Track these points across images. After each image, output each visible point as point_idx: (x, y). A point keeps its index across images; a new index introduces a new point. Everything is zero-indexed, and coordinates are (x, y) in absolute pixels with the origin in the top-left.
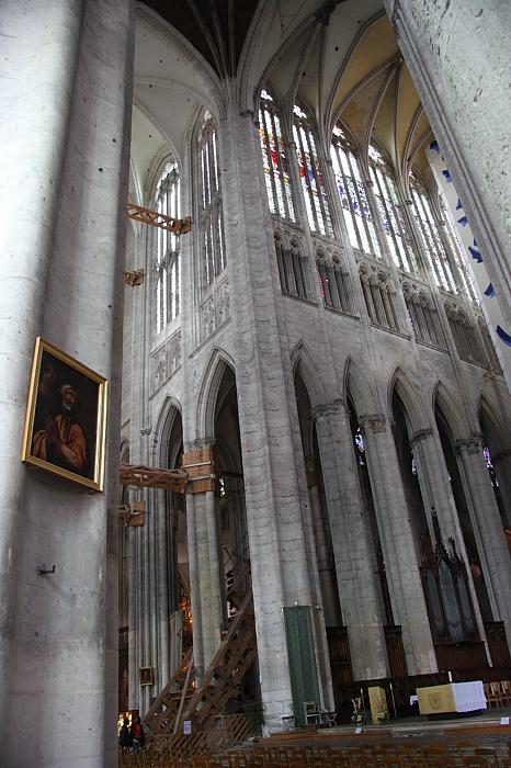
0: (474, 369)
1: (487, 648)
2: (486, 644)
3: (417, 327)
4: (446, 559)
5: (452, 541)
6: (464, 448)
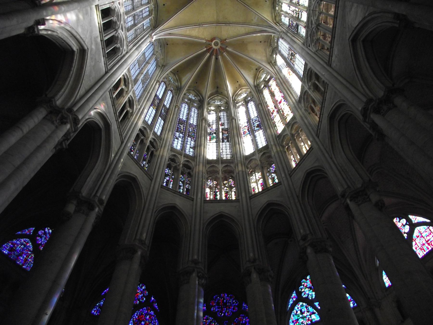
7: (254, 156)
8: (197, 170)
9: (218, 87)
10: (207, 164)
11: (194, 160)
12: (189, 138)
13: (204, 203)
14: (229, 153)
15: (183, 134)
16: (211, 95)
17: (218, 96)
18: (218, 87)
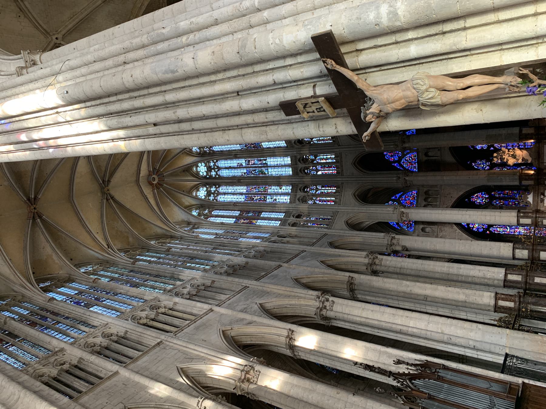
0: (272, 276)
1: (532, 382)
2: (526, 381)
3: (211, 301)
4: (412, 377)
5: (399, 362)
6: (324, 312)
11: (297, 185)
12: (269, 190)
14: (282, 159)
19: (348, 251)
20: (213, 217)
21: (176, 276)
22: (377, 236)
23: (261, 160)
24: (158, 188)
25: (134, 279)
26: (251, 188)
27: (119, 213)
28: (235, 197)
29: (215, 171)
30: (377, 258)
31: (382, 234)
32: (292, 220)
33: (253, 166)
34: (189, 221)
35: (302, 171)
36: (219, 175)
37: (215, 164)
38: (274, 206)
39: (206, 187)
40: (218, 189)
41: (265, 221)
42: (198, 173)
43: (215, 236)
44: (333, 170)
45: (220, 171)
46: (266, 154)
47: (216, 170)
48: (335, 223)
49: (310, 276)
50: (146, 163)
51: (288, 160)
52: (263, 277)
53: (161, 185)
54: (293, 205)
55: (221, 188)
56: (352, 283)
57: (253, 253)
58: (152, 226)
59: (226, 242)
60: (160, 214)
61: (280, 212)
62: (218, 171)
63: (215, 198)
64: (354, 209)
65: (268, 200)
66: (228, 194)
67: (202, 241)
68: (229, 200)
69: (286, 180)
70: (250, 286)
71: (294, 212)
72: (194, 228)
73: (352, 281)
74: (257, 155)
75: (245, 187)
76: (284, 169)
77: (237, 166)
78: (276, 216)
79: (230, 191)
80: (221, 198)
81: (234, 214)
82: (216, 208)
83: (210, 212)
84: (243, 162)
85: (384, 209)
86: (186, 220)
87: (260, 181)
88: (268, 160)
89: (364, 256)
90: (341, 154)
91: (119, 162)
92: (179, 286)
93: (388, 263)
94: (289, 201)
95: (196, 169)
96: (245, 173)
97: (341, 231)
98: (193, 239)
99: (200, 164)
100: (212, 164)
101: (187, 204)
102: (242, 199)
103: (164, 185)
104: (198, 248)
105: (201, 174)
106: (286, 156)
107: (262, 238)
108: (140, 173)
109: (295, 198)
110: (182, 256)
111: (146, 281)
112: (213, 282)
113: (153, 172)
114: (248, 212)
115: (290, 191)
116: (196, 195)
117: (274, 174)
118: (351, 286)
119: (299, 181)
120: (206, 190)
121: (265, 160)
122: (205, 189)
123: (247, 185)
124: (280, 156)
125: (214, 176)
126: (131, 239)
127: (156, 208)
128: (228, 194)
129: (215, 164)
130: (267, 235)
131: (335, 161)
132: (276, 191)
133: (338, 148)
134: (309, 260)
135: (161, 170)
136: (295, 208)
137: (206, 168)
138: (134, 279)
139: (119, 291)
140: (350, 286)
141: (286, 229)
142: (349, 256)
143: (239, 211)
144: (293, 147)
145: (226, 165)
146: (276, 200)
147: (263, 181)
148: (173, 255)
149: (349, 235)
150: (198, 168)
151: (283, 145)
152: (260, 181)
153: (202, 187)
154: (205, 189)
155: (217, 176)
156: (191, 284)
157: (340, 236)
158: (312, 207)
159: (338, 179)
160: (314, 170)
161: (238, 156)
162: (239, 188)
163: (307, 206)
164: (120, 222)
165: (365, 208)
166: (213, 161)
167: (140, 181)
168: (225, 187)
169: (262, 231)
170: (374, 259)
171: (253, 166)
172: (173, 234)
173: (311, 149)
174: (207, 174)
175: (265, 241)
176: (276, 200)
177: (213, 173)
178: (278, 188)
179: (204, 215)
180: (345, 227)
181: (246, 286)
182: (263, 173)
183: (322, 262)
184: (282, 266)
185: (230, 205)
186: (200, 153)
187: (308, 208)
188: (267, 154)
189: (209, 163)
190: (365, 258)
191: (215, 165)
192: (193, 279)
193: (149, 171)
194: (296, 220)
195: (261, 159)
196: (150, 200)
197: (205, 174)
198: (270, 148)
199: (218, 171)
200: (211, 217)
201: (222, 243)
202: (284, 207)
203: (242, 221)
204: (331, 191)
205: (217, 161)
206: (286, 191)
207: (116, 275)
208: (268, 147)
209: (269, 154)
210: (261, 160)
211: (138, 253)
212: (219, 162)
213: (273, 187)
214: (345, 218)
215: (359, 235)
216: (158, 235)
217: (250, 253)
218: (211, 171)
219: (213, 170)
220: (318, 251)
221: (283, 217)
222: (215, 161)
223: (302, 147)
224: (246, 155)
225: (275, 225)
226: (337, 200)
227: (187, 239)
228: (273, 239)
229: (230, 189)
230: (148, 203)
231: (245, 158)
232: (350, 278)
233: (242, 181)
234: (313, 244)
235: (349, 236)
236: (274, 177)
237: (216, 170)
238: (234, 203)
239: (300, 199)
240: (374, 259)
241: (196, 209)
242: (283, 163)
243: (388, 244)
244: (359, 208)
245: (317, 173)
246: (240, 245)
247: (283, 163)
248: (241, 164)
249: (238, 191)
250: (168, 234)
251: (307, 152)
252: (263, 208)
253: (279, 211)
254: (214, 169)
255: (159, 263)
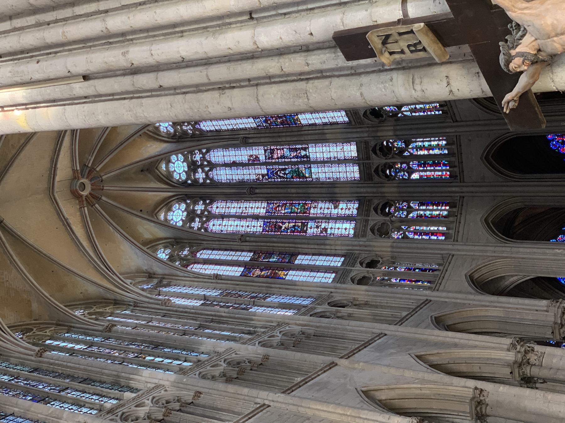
0: (317, 384)
7: (358, 113)
8: (397, 195)
9: (142, 171)
10: (372, 180)
12: (312, 211)
13: (464, 182)
15: (308, 223)
16: (160, 179)
17: (156, 168)
18: (142, 171)
19: (472, 336)
20: (198, 263)
21: (123, 382)
22: (535, 305)
23: (296, 150)
24: (91, 205)
25: (41, 387)
26: (276, 206)
27: (12, 253)
28: (243, 223)
29: (203, 171)
30: (533, 350)
31: (544, 302)
32: (359, 270)
33: (280, 160)
34: (151, 271)
35: (381, 173)
36: (212, 180)
37: (204, 157)
38: (322, 241)
39: (187, 204)
40: (209, 208)
41: (304, 273)
42: (169, 175)
43: (202, 302)
44: (441, 171)
45: (214, 172)
46: (306, 138)
47: (207, 169)
48: (446, 278)
49: (394, 386)
50: (68, 154)
51: (351, 150)
52: (298, 386)
53: (98, 199)
54: (362, 241)
55: (215, 206)
56: (481, 401)
57: (279, 337)
58: (79, 279)
59: (223, 314)
60: (94, 257)
61: (334, 255)
62: (210, 170)
63: (202, 225)
64: (486, 251)
65: (309, 231)
66: (229, 216)
67: (176, 311)
68: (230, 229)
69: (348, 190)
70: (271, 404)
71: (363, 256)
72: (160, 284)
73: (482, 398)
74: (288, 139)
75: (265, 205)
76: (342, 168)
77: (249, 160)
78: (325, 264)
79: (233, 211)
80: (215, 226)
81: (241, 259)
82: (206, 246)
83: (193, 253)
84: (260, 152)
85: (547, 251)
86: (145, 268)
87: (293, 191)
88: (310, 149)
89: (506, 347)
90: (458, 137)
91: (14, 152)
92: (129, 401)
93: (555, 361)
94: (352, 232)
95: (167, 167)
96: (263, 176)
97: (460, 296)
98: (158, 307)
99: (174, 158)
100: (198, 157)
101: (147, 236)
102: (257, 227)
103: (103, 198)
104: (169, 326)
105: (176, 176)
106: (347, 141)
107: (297, 308)
108: (55, 175)
109: (365, 226)
110: (136, 340)
111: (63, 391)
112: (198, 394)
113: (82, 171)
114: (270, 254)
115: (355, 212)
116: (166, 219)
117: (322, 176)
118: (478, 409)
119: (374, 193)
120: (186, 210)
121: (305, 149)
122: (183, 206)
123: (268, 199)
124: (335, 141)
125: (201, 181)
126: (35, 306)
127: (85, 243)
128: (229, 216)
129: (204, 157)
130: (306, 302)
131: (446, 152)
132: (326, 211)
133: (452, 127)
134: (392, 354)
135: (98, 169)
136: (366, 246)
137: (185, 164)
138: (41, 387)
139: (10, 410)
140: (476, 407)
141: (346, 289)
142: (475, 347)
143: (250, 251)
144: (361, 123)
145: (227, 160)
146: (325, 229)
147: (300, 191)
148: (117, 339)
149: (475, 303)
150: (171, 165)
151: (340, 120)
152: (293, 191)
153: (177, 202)
154: (183, 206)
155: (208, 181)
156: (154, 398)
157: (456, 304)
158: (399, 245)
159: (454, 189)
160: (404, 171)
161: (251, 141)
162: (251, 205)
163: (389, 244)
164: (14, 271)
165: (508, 249)
166: (200, 150)
167: (56, 189)
168: (223, 204)
169: (298, 293)
170: (526, 352)
171: (280, 160)
172: (119, 297)
173: (398, 127)
174: (188, 177)
175: (304, 314)
176: (325, 229)
177: (200, 175)
178: (331, 205)
179: (181, 259)
180: (466, 286)
181: (264, 405)
182: (299, 174)
183: (419, 357)
184: (336, 365)
185: (233, 240)
186: (175, 135)
187: (392, 247)
188: (309, 137)
189: (192, 155)
190: (508, 350)
191: (203, 159)
192: (157, 387)
193: (74, 171)
194: (368, 272)
195: (297, 147)
196: (74, 228)
197: (184, 177)
198: (315, 125)
199: (210, 170)
200: (195, 263)
201: (215, 316)
202: (342, 245)
203: (258, 272)
204: (438, 213)
205: (208, 151)
206: (347, 212)
207: (6, 377)
208: (310, 122)
209: (313, 137)
210: (296, 150)
211: (48, 334)
212: (212, 153)
213: (321, 205)
214: (466, 270)
215: (495, 304)
216: (88, 299)
217: (273, 336)
218: (195, 171)
219: (200, 170)
220: (411, 335)
221: (339, 264)
222: (204, 151)
223: (380, 122)
224: (267, 140)
225: (324, 280)
226: (450, 231)
227: (148, 308)
228: (320, 309)
229: (234, 208)
230: (70, 235)
231: (264, 146)
232: (478, 392)
233: (257, 191)
234: (401, 321)
235: (475, 306)
236: (323, 183)
237: (207, 169)
238: (242, 236)
239: (376, 228)
240: (526, 352)
241: (165, 247)
242: (342, 155)
243: (555, 323)
244: (497, 249)
245: (410, 176)
246: (252, 320)
247: (341, 156)
248: (257, 157)
249: (250, 211)
250: (108, 295)
251: (391, 133)
252: (299, 246)
253: (333, 252)
254: (202, 166)
255: (91, 355)
